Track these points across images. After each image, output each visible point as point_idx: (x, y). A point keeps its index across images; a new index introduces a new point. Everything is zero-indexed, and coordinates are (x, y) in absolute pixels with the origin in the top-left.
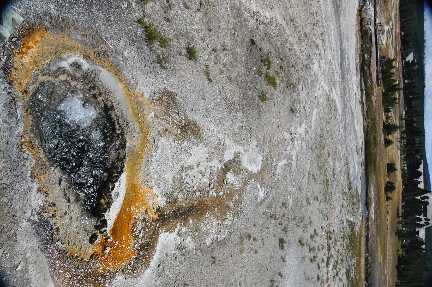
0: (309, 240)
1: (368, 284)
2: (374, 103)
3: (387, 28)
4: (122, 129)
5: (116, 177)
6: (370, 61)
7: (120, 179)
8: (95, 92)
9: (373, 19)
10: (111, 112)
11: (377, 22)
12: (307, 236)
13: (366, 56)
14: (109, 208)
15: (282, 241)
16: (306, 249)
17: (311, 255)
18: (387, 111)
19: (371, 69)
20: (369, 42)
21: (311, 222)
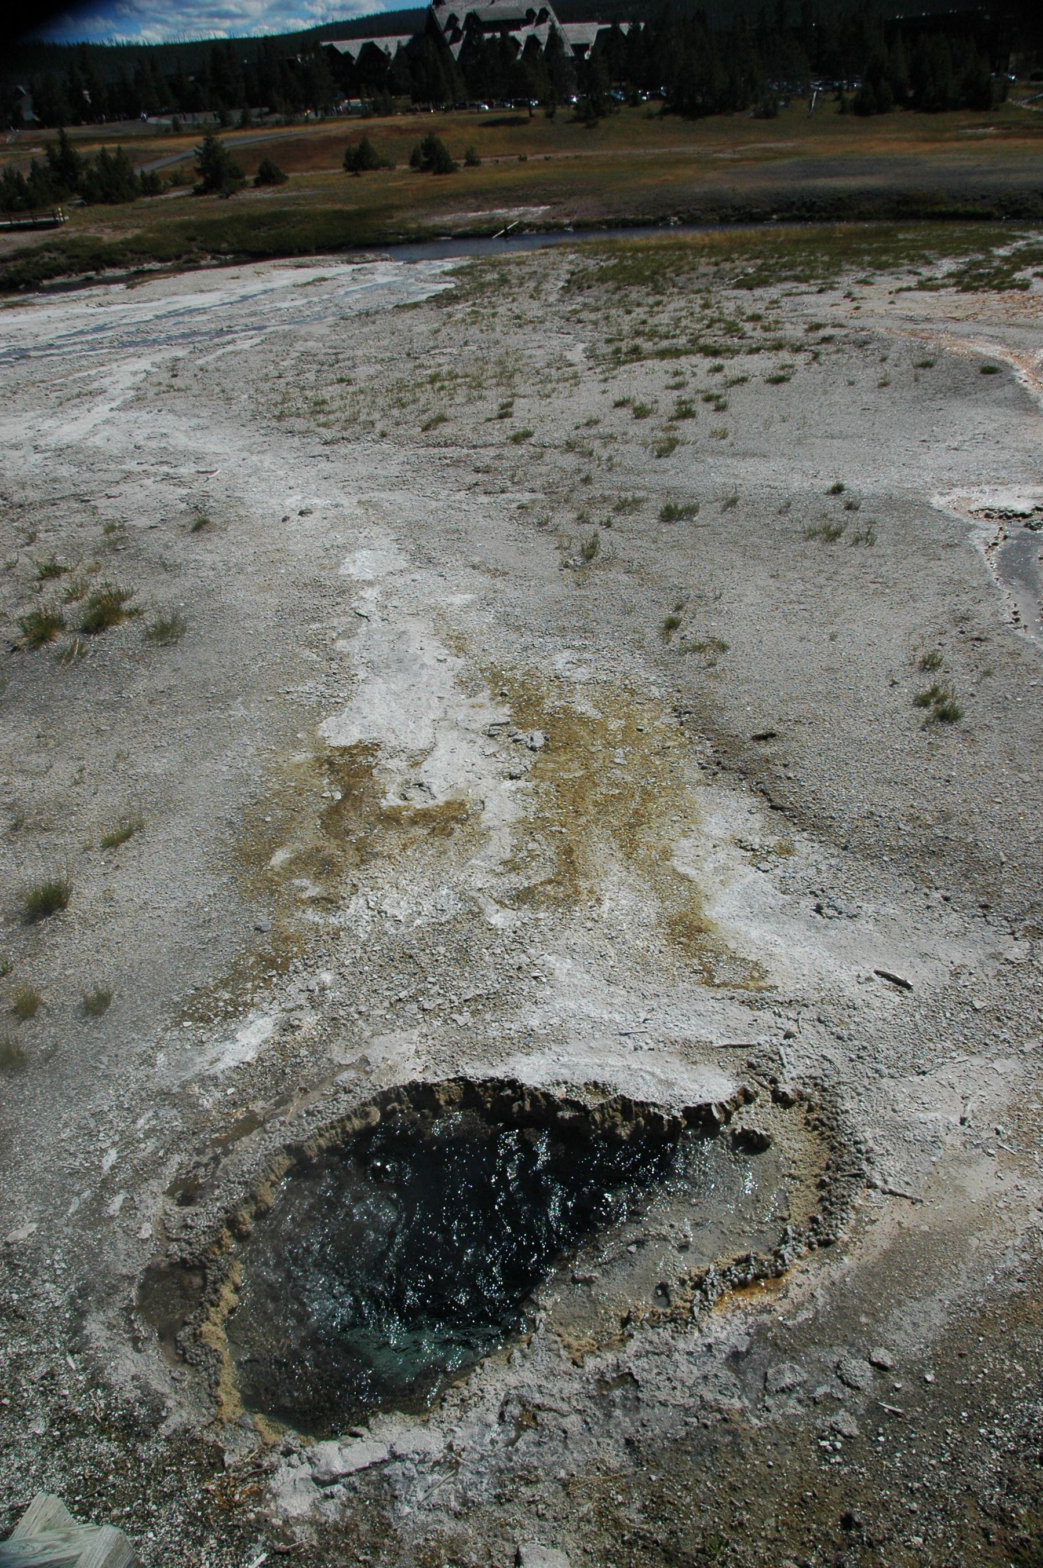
0: (650, 421)
2: (129, 235)
4: (364, 1104)
5: (534, 1099)
7: (539, 1086)
8: (247, 1216)
10: (309, 1153)
12: (642, 429)
14: (642, 1104)
15: (669, 515)
16: (687, 428)
17: (702, 409)
18: (151, 186)
21: (591, 423)
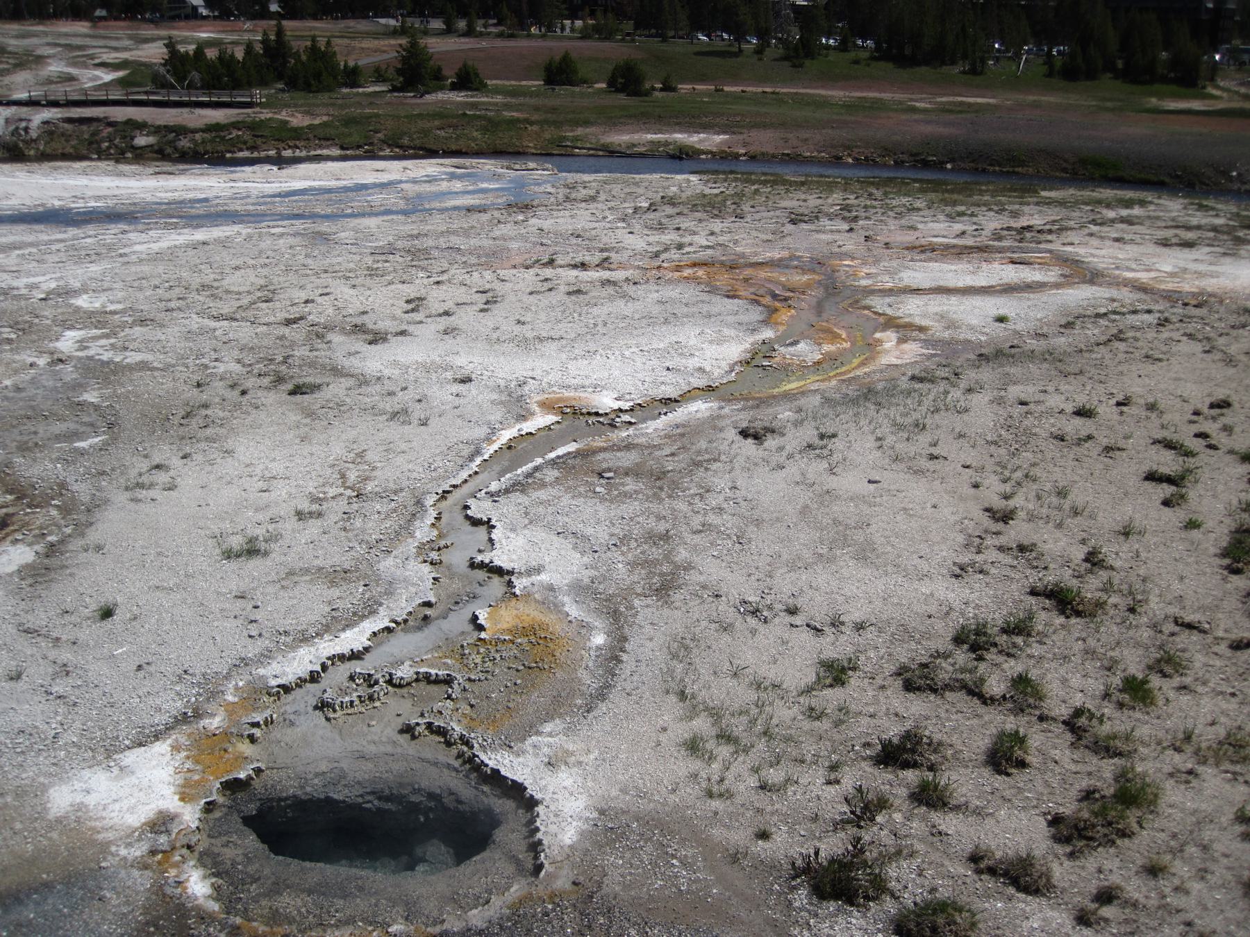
1: (952, 160)
2: (317, 122)
3: (55, 68)
6: (157, 130)
9: (14, 109)
11: (23, 96)
13: (141, 141)
18: (352, 77)
19: (191, 125)
20: (94, 126)
